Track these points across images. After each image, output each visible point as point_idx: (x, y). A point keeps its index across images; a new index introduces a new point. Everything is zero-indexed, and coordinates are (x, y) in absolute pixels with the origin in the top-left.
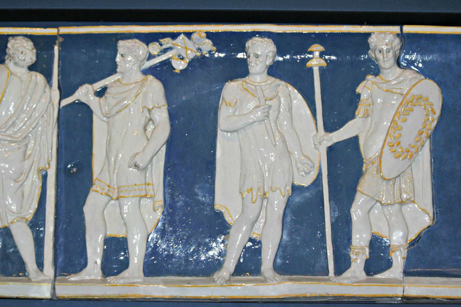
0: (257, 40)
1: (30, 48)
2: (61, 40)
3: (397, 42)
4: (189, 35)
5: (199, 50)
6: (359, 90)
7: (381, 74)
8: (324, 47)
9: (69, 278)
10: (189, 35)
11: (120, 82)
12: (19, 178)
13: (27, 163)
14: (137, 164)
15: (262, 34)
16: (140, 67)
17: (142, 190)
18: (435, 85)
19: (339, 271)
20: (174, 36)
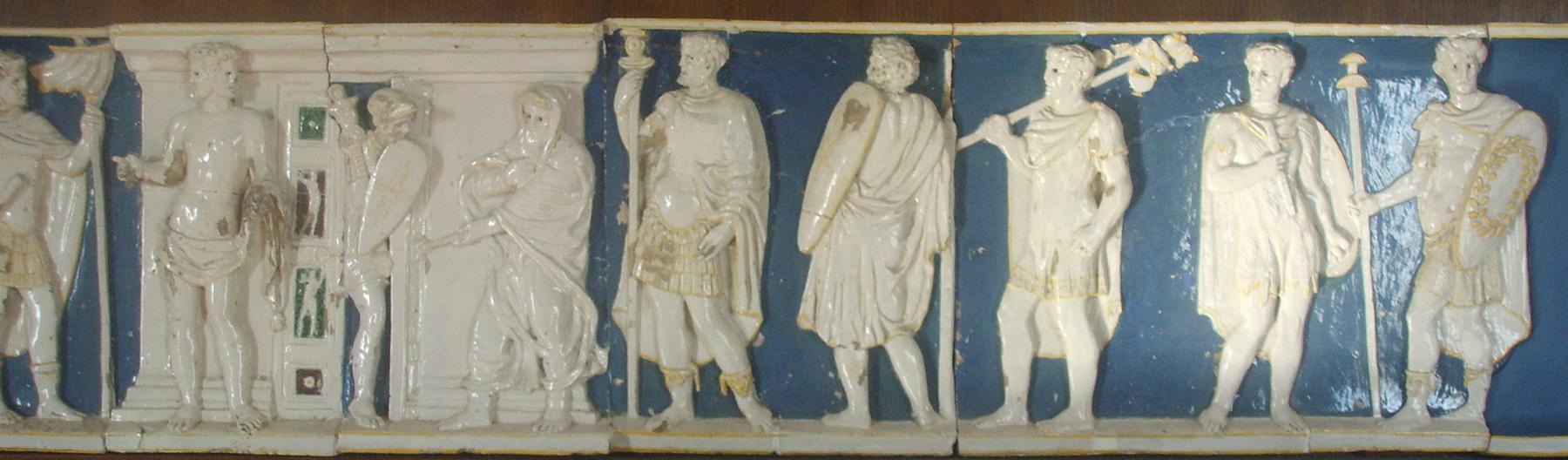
4: (1158, 38)
5: (1172, 61)
15: (1274, 39)
20: (1135, 39)
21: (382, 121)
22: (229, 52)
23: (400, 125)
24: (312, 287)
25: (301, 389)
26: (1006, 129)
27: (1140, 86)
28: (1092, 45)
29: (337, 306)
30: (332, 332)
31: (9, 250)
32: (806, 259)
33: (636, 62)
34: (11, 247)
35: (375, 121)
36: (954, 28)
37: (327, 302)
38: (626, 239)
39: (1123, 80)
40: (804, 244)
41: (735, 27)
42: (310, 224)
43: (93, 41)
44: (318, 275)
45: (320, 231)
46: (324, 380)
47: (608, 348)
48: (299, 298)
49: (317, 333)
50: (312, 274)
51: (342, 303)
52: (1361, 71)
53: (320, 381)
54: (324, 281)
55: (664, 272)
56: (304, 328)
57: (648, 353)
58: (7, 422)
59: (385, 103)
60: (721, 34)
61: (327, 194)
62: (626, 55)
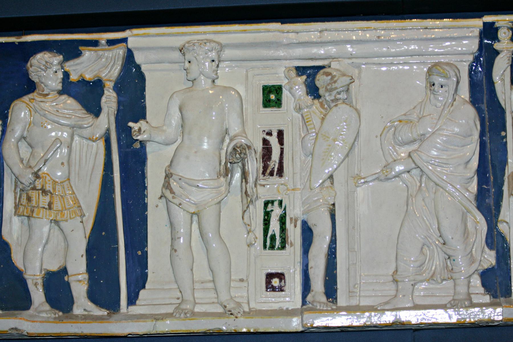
21: (327, 90)
22: (213, 45)
23: (339, 93)
24: (276, 212)
25: (269, 287)
29: (295, 226)
30: (292, 245)
31: (51, 193)
34: (52, 191)
35: (321, 92)
37: (289, 225)
38: (506, 171)
42: (274, 168)
43: (111, 43)
44: (281, 203)
45: (280, 172)
46: (287, 281)
47: (496, 249)
48: (267, 222)
49: (280, 246)
50: (276, 204)
51: (299, 224)
53: (283, 281)
54: (285, 209)
56: (271, 243)
58: (53, 316)
59: (330, 77)
61: (285, 147)
62: (499, 41)
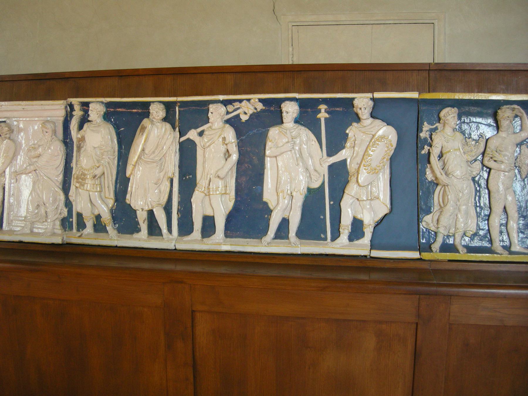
0: (287, 103)
1: (161, 109)
2: (179, 104)
3: (371, 103)
4: (249, 100)
5: (256, 109)
6: (347, 132)
7: (361, 122)
8: (327, 106)
9: (183, 239)
10: (249, 100)
11: (211, 128)
12: (158, 182)
13: (162, 174)
14: (219, 176)
16: (222, 119)
17: (223, 190)
18: (393, 129)
19: (334, 239)
20: (240, 101)
26: (196, 134)
27: (244, 118)
28: (226, 103)
32: (129, 179)
33: (78, 113)
36: (177, 99)
39: (238, 116)
40: (127, 175)
41: (106, 100)
52: (326, 111)
55: (82, 183)
57: (79, 210)
60: (102, 102)
62: (75, 111)
